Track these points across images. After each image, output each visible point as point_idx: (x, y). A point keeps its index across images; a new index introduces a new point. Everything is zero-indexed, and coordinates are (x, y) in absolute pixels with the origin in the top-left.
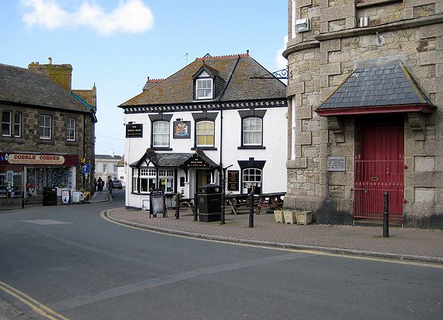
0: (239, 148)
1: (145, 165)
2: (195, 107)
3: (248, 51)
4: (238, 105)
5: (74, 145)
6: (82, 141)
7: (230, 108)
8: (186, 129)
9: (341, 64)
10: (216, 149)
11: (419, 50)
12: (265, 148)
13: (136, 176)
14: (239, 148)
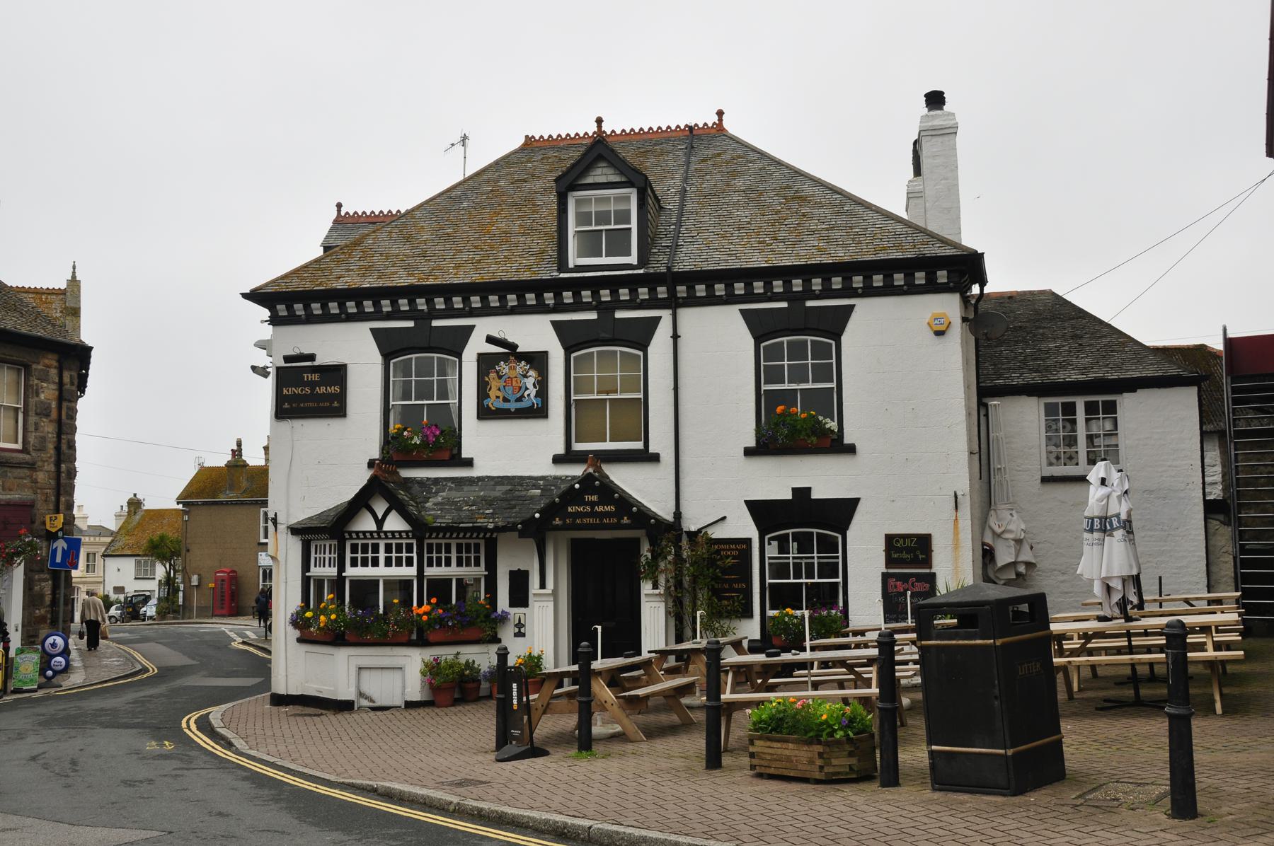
0: (748, 452)
1: (366, 523)
3: (720, 114)
4: (739, 288)
5: (19, 465)
7: (711, 300)
8: (530, 382)
10: (655, 458)
12: (851, 449)
14: (748, 452)
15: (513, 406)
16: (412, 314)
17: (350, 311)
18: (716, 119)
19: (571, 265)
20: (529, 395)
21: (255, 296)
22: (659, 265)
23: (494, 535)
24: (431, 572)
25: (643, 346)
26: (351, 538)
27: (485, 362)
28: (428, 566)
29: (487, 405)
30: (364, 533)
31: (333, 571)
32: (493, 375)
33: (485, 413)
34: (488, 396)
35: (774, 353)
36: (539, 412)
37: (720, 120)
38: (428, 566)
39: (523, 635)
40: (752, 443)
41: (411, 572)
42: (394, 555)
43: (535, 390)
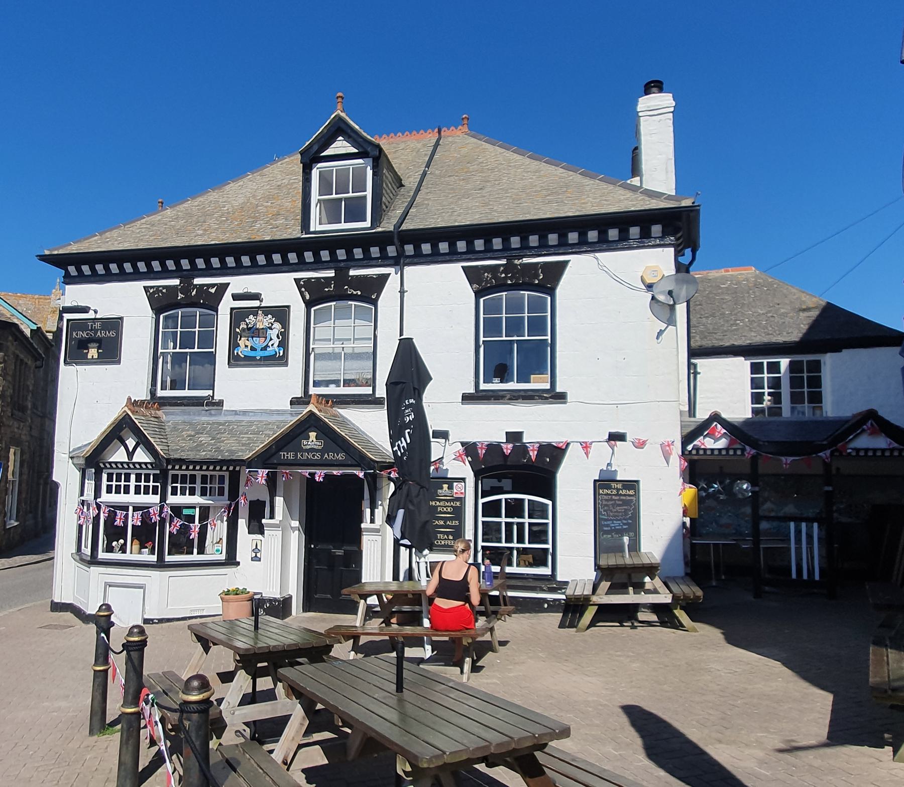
0: (467, 398)
1: (120, 456)
2: (309, 256)
7: (436, 258)
8: (273, 333)
12: (561, 397)
14: (467, 398)
15: (259, 354)
16: (179, 272)
19: (312, 229)
20: (272, 345)
22: (387, 225)
23: (238, 468)
24: (172, 500)
27: (237, 316)
28: (172, 494)
29: (237, 353)
30: (116, 463)
31: (156, 499)
33: (234, 360)
36: (281, 360)
38: (172, 494)
39: (260, 560)
41: (156, 499)
42: (143, 484)
43: (278, 340)
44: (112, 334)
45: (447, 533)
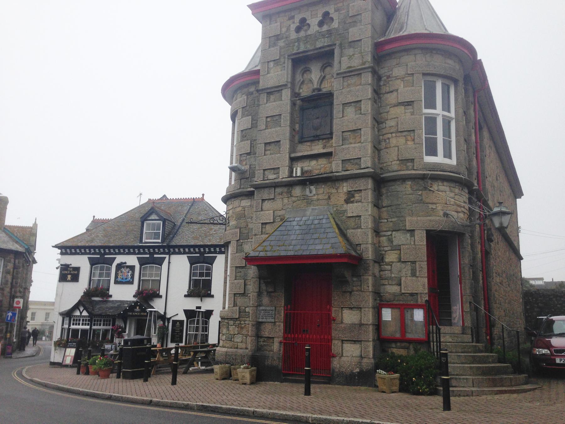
0: (185, 296)
1: (77, 313)
2: (142, 250)
3: (203, 195)
6: (9, 285)
7: (180, 253)
8: (130, 274)
9: (274, 212)
10: (161, 297)
11: (347, 201)
13: (66, 326)
14: (185, 296)
15: (124, 281)
17: (83, 252)
18: (202, 196)
19: (143, 242)
21: (56, 246)
24: (94, 327)
25: (161, 265)
26: (73, 317)
30: (76, 316)
32: (120, 272)
34: (118, 277)
35: (196, 268)
36: (131, 283)
37: (203, 197)
40: (187, 294)
41: (88, 327)
44: (76, 272)
45: (178, 337)
